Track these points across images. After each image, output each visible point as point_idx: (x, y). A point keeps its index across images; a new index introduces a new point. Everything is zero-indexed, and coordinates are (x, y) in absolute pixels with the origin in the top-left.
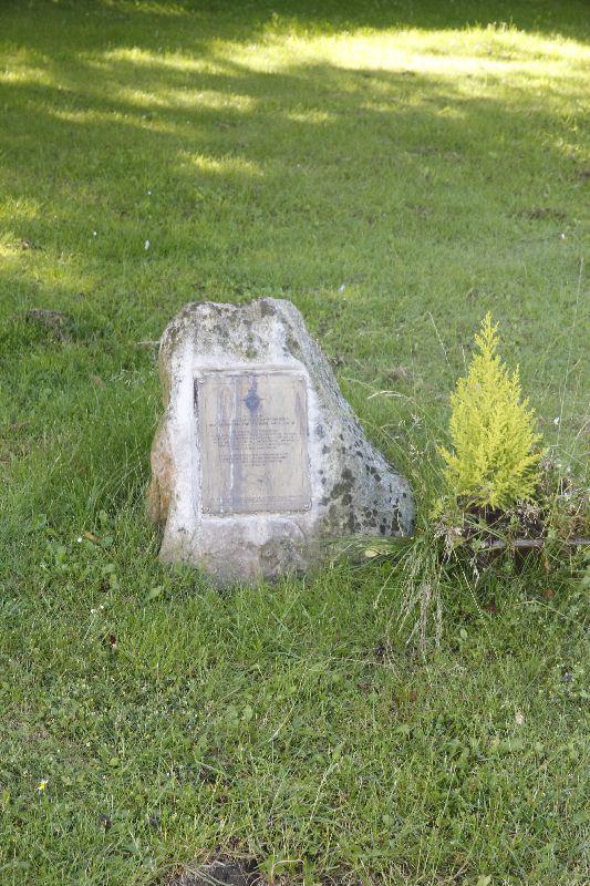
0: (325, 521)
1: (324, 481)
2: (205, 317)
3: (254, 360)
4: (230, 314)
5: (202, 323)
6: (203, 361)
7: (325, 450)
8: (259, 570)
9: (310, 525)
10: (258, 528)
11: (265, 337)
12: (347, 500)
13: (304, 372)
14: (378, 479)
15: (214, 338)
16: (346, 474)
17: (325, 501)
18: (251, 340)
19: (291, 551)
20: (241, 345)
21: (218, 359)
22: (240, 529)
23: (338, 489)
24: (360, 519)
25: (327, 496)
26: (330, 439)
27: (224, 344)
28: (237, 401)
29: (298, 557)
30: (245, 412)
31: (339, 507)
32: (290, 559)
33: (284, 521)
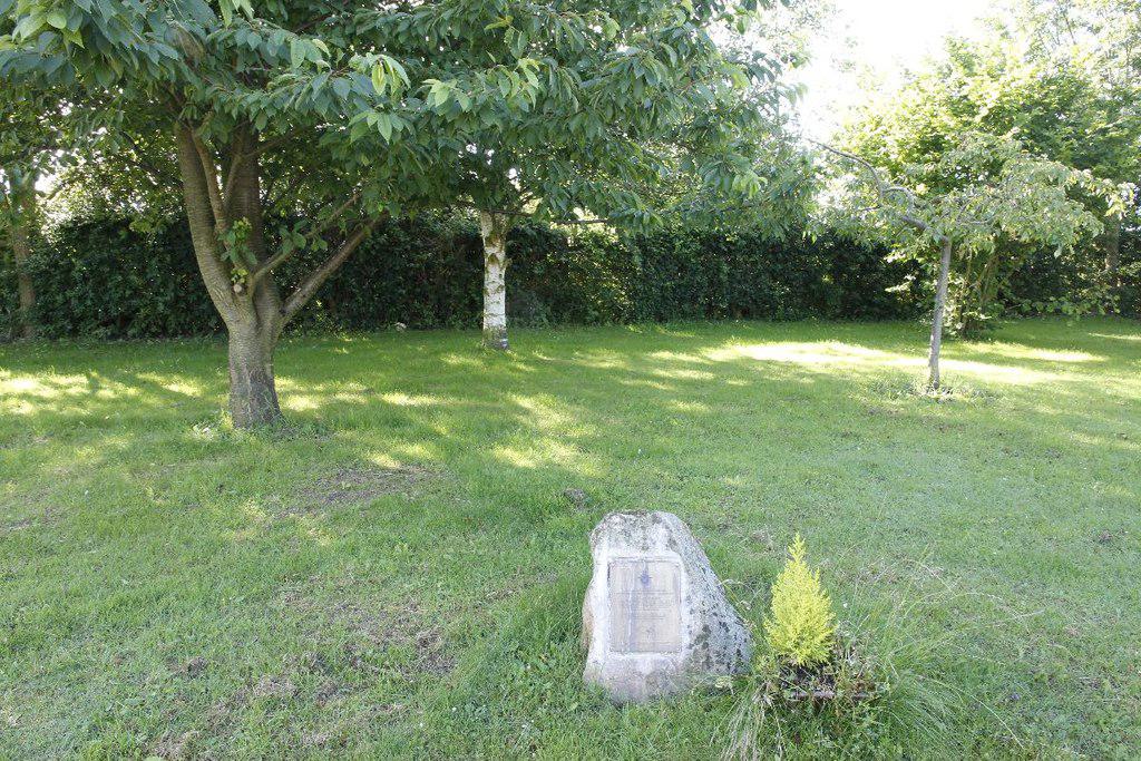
1: (690, 633)
6: (615, 552)
7: (692, 612)
8: (645, 692)
10: (646, 663)
12: (706, 646)
13: (678, 560)
14: (727, 630)
15: (621, 537)
16: (706, 628)
17: (690, 647)
22: (634, 662)
23: (700, 638)
24: (714, 659)
26: (696, 604)
27: (628, 541)
29: (671, 683)
30: (640, 586)
32: (666, 684)
33: (663, 659)
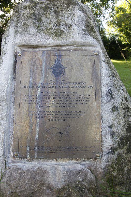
0: (112, 166)
1: (113, 134)
2: (25, 8)
3: (60, 38)
4: (43, 6)
5: (23, 12)
6: (21, 39)
7: (114, 109)
9: (100, 170)
11: (69, 21)
15: (30, 22)
17: (113, 151)
18: (58, 24)
19: (83, 192)
20: (51, 28)
21: (32, 37)
22: (41, 172)
25: (115, 146)
26: (118, 100)
27: (38, 27)
28: (46, 69)
30: (52, 77)
31: (124, 155)
33: (79, 167)
